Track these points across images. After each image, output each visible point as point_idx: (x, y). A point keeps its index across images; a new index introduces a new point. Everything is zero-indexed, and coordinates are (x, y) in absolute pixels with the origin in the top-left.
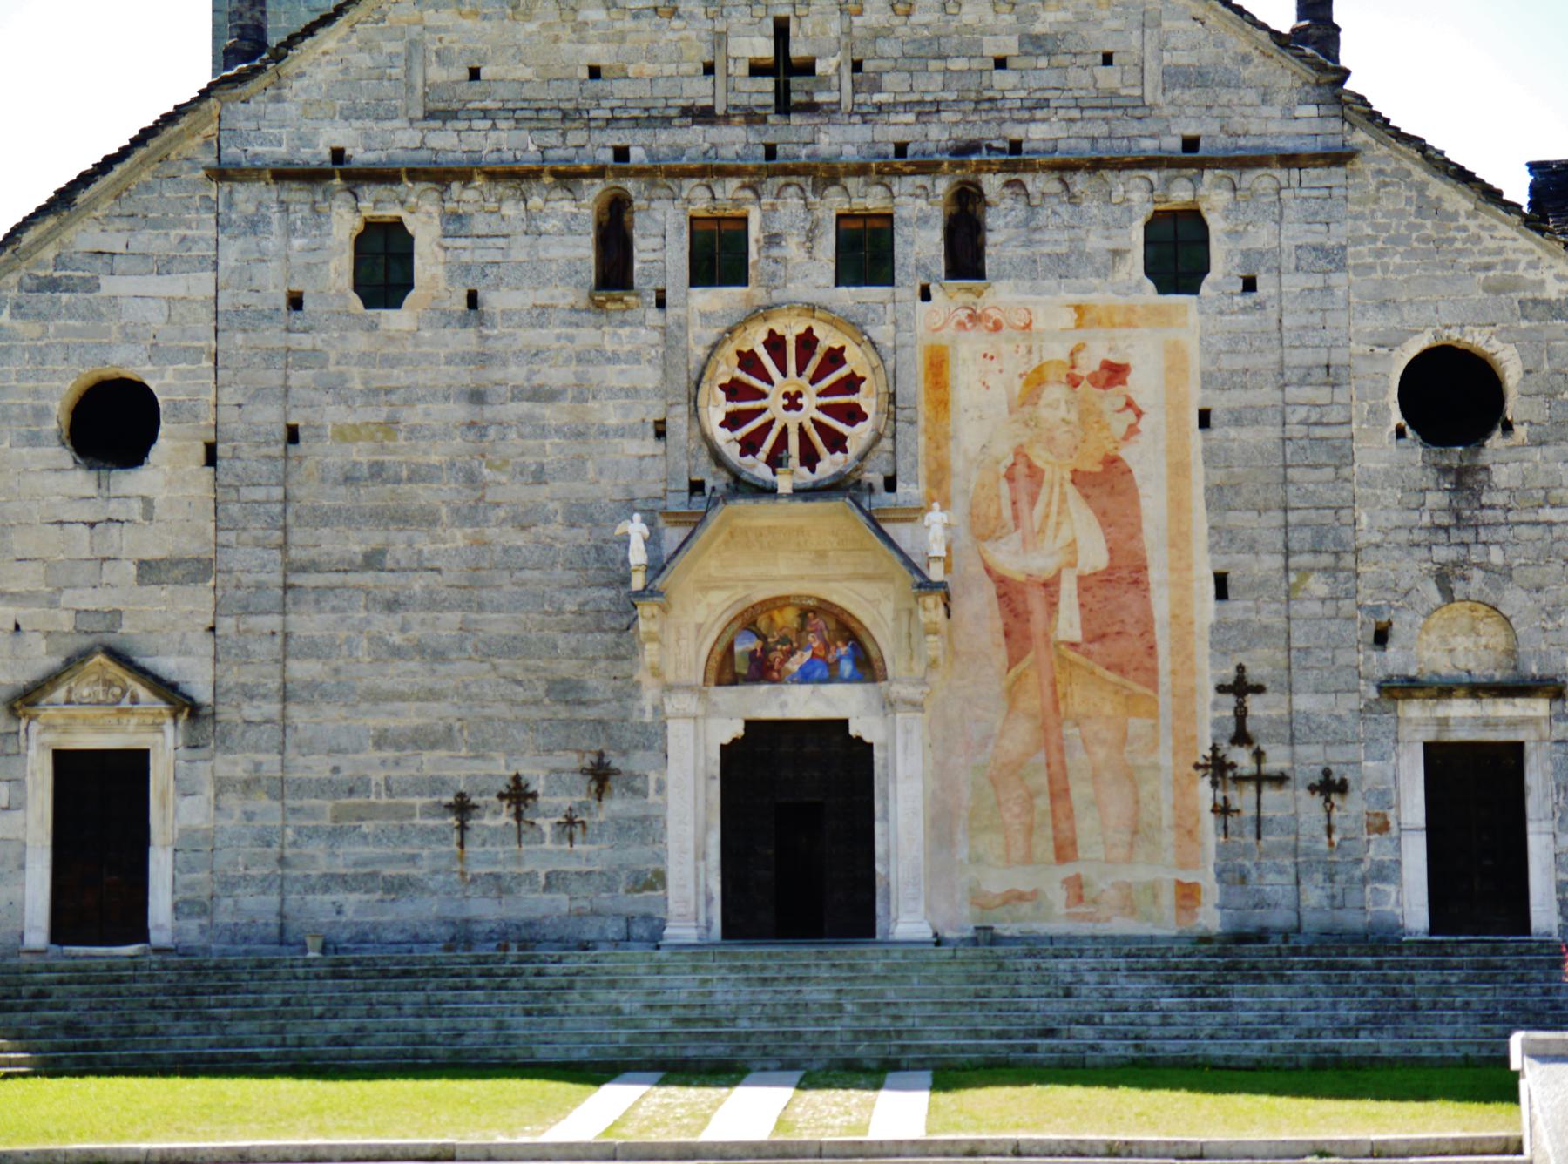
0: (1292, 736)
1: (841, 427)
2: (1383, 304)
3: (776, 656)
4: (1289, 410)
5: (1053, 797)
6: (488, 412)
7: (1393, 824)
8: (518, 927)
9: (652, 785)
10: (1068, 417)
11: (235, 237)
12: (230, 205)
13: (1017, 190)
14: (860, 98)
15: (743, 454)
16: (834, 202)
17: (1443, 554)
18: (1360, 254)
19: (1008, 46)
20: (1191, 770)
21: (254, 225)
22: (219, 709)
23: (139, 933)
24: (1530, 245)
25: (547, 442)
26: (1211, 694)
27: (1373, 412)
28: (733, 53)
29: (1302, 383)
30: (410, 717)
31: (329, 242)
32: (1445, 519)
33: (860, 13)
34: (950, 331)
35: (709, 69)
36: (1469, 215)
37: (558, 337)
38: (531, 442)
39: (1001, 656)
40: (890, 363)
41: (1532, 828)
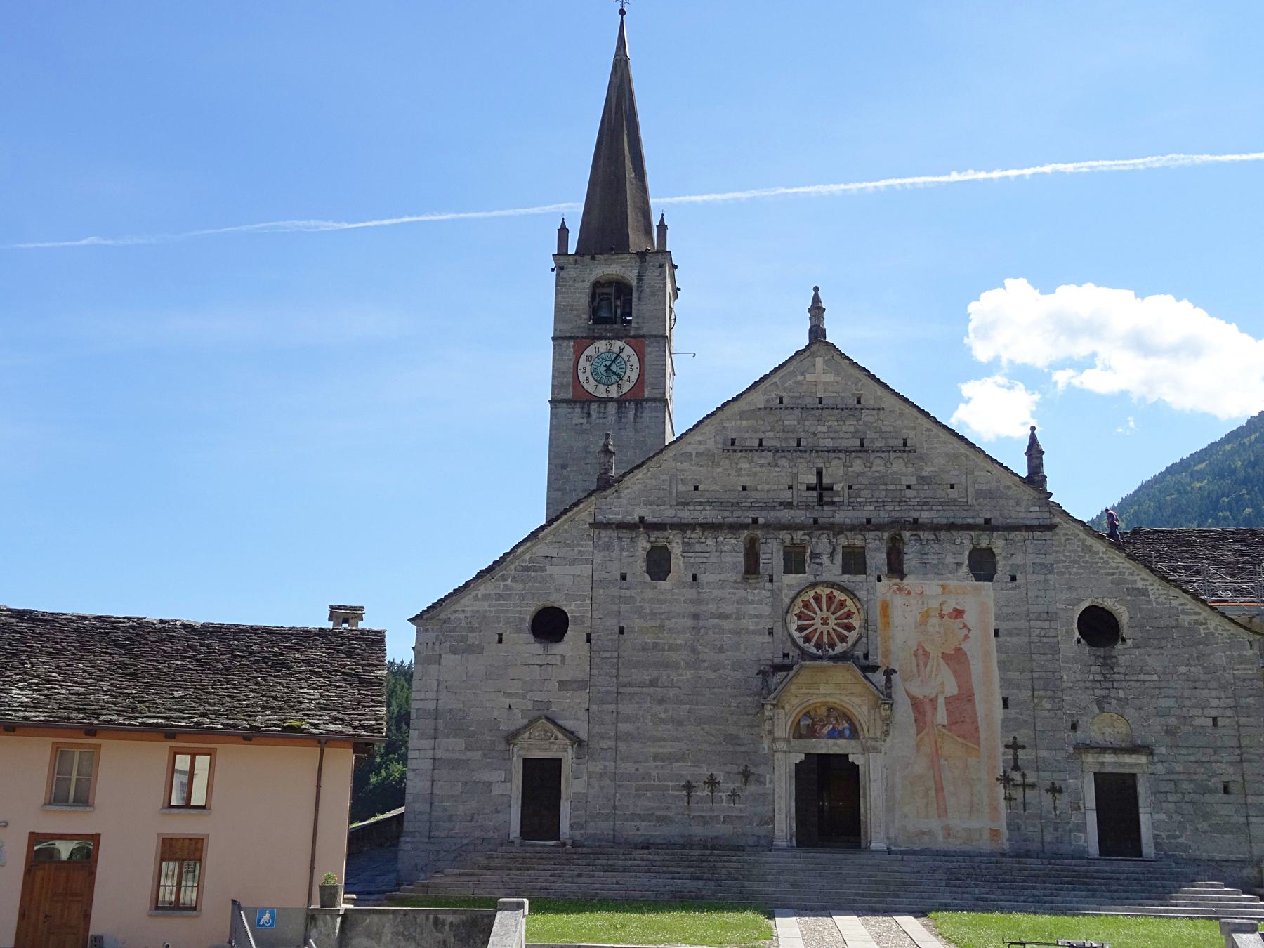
0: (1038, 768)
1: (845, 632)
2: (1070, 588)
4: (1032, 630)
5: (937, 791)
6: (701, 623)
7: (1082, 806)
11: (600, 551)
12: (599, 538)
13: (916, 538)
14: (852, 500)
15: (805, 642)
16: (842, 540)
17: (1098, 692)
18: (1059, 567)
19: (912, 481)
21: (608, 547)
22: (590, 743)
23: (556, 836)
24: (1130, 566)
25: (725, 636)
26: (1002, 749)
27: (1067, 632)
28: (799, 481)
29: (1036, 620)
30: (667, 748)
31: (637, 554)
32: (1099, 678)
33: (851, 466)
34: (889, 595)
35: (790, 488)
36: (1103, 553)
37: (729, 593)
38: (718, 636)
39: (913, 730)
40: (865, 606)
41: (1141, 810)
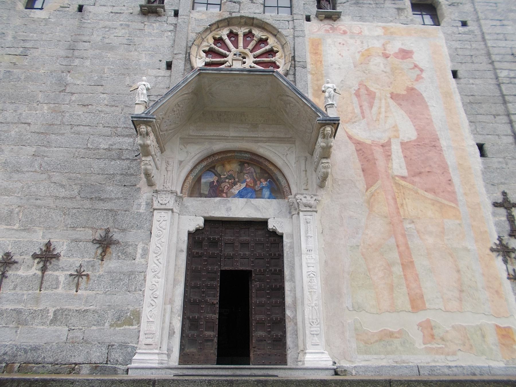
3: (225, 186)
5: (404, 266)
8: (26, 352)
9: (140, 251)
10: (385, 70)
20: (488, 251)
26: (490, 208)
40: (290, 45)
